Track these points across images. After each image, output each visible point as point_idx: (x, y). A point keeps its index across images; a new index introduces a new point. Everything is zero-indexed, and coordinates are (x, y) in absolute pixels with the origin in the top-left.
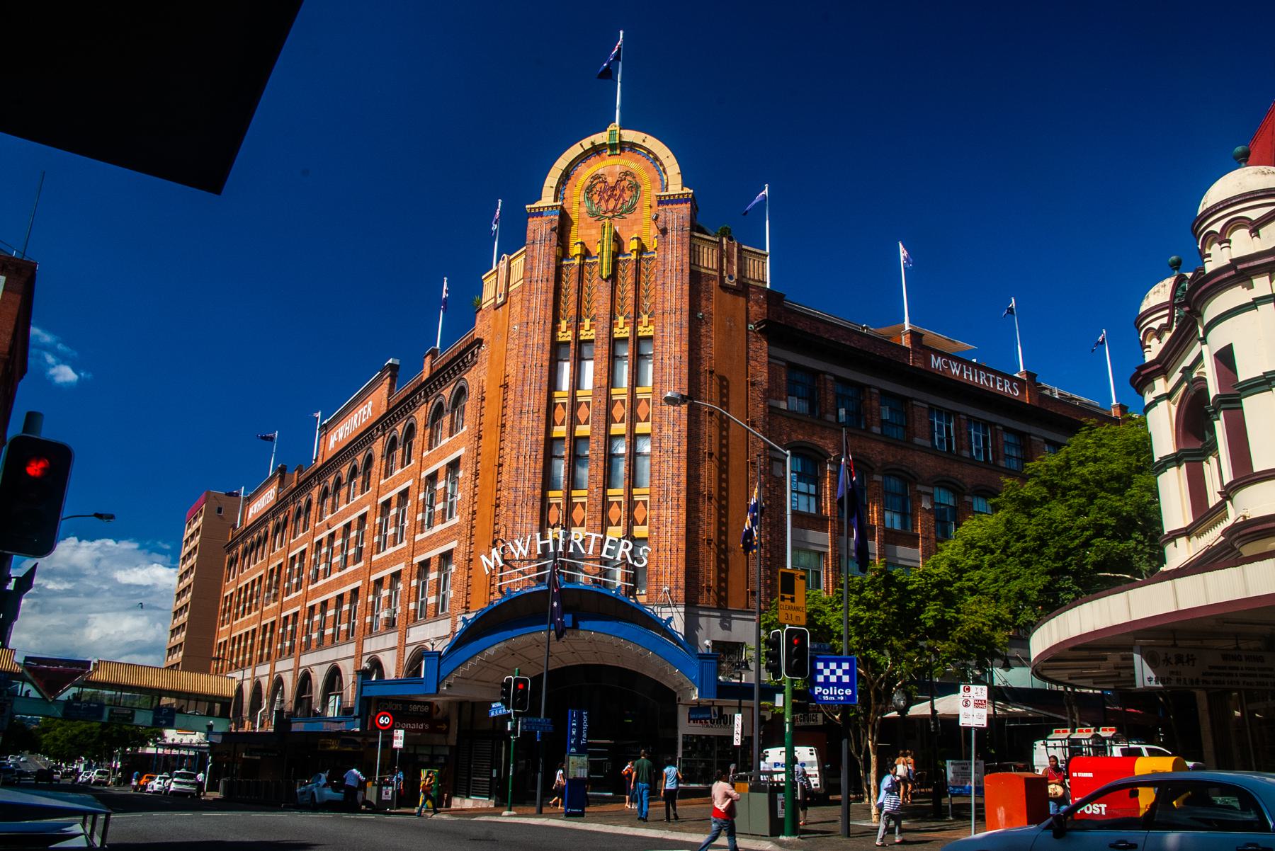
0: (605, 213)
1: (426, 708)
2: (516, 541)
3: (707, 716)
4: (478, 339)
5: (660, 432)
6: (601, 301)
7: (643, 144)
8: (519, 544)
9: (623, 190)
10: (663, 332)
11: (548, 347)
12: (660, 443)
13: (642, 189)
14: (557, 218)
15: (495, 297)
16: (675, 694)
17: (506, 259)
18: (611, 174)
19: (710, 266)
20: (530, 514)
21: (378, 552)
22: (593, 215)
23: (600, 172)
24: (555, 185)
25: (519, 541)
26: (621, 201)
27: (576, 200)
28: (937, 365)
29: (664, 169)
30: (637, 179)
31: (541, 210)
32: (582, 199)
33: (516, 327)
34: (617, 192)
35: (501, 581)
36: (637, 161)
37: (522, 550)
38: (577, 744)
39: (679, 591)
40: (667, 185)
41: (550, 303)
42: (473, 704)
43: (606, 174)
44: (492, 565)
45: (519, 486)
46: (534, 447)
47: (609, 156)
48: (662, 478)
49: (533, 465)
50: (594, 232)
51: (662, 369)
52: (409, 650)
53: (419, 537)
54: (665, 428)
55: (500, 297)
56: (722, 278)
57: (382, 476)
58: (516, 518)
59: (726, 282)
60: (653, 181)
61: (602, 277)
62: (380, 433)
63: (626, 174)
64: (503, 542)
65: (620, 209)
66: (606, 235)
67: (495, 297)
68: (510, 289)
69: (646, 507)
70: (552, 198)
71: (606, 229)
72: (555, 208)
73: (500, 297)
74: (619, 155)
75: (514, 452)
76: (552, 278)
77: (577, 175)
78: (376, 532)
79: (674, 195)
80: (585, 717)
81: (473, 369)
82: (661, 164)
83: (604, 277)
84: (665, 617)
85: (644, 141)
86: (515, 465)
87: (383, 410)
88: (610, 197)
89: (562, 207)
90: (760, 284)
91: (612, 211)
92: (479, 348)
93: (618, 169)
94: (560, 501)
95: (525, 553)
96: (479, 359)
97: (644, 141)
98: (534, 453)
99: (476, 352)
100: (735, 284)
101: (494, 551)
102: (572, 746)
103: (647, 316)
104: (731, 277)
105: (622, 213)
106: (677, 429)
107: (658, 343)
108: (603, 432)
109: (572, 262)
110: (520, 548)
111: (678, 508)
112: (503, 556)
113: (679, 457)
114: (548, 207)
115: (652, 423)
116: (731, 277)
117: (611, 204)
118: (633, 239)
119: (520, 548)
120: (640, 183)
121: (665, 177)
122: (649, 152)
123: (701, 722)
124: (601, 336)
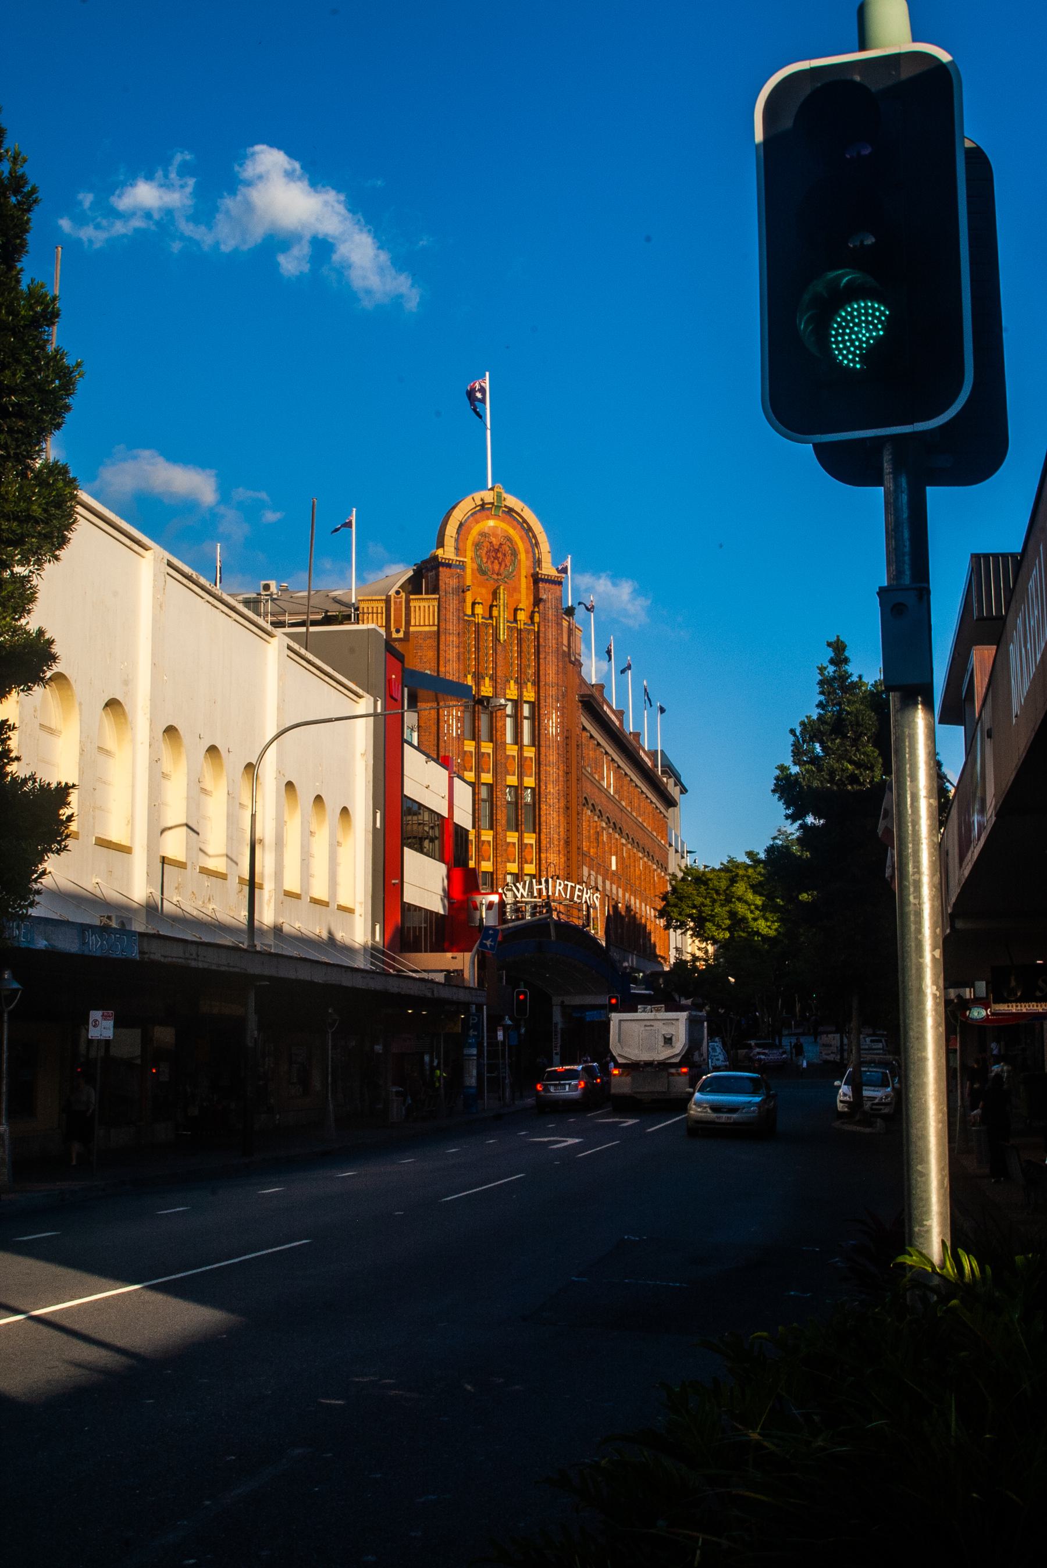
2: (518, 884)
7: (522, 513)
18: (495, 535)
26: (503, 565)
29: (537, 544)
31: (450, 562)
34: (499, 555)
43: (490, 533)
48: (548, 827)
55: (398, 631)
60: (527, 552)
72: (461, 564)
73: (398, 631)
82: (535, 537)
85: (522, 510)
95: (525, 894)
97: (522, 510)
106: (557, 788)
110: (521, 890)
119: (521, 890)
122: (525, 521)
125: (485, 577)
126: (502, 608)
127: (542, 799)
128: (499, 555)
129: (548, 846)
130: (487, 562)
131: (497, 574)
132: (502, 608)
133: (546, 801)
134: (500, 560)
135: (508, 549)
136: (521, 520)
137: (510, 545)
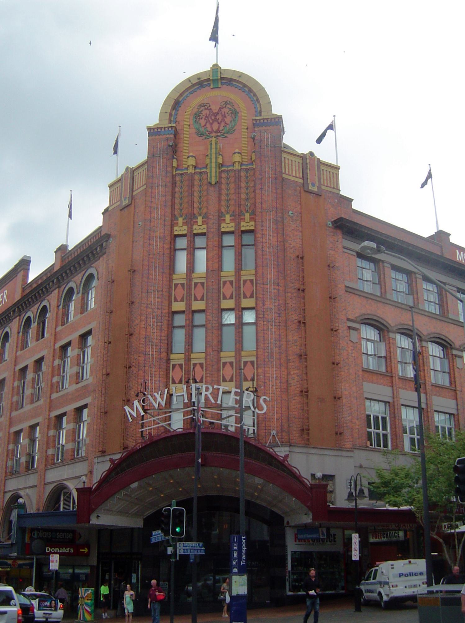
1: (70, 536)
3: (315, 536)
4: (106, 234)
5: (263, 305)
8: (158, 397)
9: (224, 116)
10: (262, 226)
11: (168, 239)
12: (264, 315)
13: (239, 115)
14: (172, 136)
15: (121, 201)
16: (282, 519)
19: (298, 176)
20: (158, 373)
21: (17, 410)
22: (200, 134)
23: (205, 101)
24: (169, 111)
25: (158, 394)
26: (223, 124)
27: (187, 123)
28: (460, 258)
29: (258, 100)
31: (159, 130)
33: (140, 223)
34: (219, 117)
35: (142, 427)
37: (161, 401)
38: (238, 566)
39: (284, 434)
40: (260, 112)
41: (169, 203)
42: (112, 530)
44: (135, 415)
45: (147, 350)
46: (160, 318)
47: (212, 88)
49: (159, 334)
51: (263, 255)
52: (49, 489)
53: (54, 396)
54: (268, 302)
57: (19, 348)
58: (146, 377)
59: (310, 188)
61: (210, 183)
62: (16, 315)
63: (226, 103)
64: (145, 395)
65: (223, 130)
67: (121, 201)
68: (135, 193)
69: (253, 366)
70: (167, 121)
73: (125, 200)
74: (220, 88)
75: (143, 323)
76: (170, 184)
78: (15, 393)
79: (267, 119)
80: (244, 541)
81: (101, 259)
82: (255, 95)
83: (213, 183)
84: (282, 454)
86: (144, 333)
87: (18, 297)
88: (213, 121)
89: (176, 128)
90: (335, 191)
91: (216, 132)
92: (107, 241)
94: (182, 362)
95: (163, 404)
96: (107, 251)
98: (159, 324)
99: (104, 245)
101: (136, 403)
102: (235, 567)
103: (248, 214)
104: (313, 185)
105: (224, 134)
107: (259, 235)
108: (216, 306)
109: (186, 171)
110: (159, 399)
111: (280, 367)
112: (143, 406)
113: (279, 325)
114: (165, 128)
115: (257, 299)
116: (313, 185)
117: (215, 126)
119: (159, 399)
120: (237, 110)
121: (258, 106)
123: (305, 541)
124: (212, 230)
125: (203, 138)
126: (214, 156)
127: (259, 316)
129: (266, 360)
130: (205, 125)
131: (216, 132)
133: (264, 317)
134: (219, 121)
135: (228, 110)
136: (241, 86)
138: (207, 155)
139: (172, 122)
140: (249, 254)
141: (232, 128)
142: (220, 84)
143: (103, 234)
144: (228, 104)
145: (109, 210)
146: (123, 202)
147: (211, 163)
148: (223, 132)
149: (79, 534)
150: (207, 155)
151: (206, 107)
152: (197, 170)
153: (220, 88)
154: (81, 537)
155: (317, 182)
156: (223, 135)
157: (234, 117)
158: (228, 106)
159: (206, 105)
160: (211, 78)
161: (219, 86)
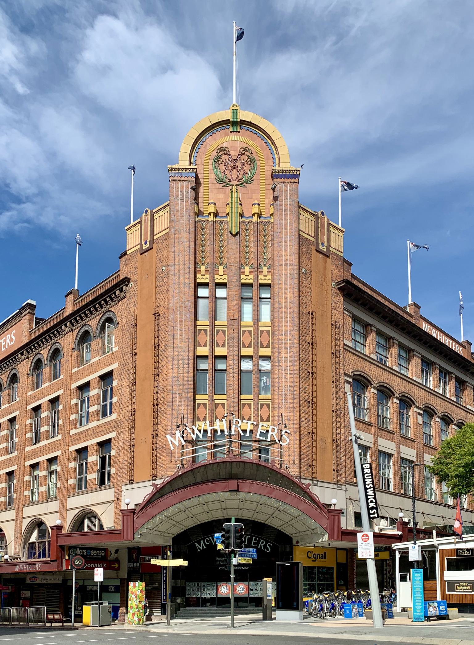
0: (230, 181)
1: (102, 553)
6: (231, 253)
15: (141, 244)
17: (149, 212)
23: (225, 145)
30: (254, 155)
32: (211, 167)
34: (238, 164)
36: (254, 140)
43: (230, 148)
47: (231, 132)
50: (221, 196)
55: (146, 243)
56: (317, 244)
59: (320, 248)
63: (245, 149)
66: (233, 199)
71: (233, 193)
74: (239, 132)
77: (206, 146)
88: (234, 167)
93: (239, 145)
100: (325, 250)
104: (323, 244)
116: (323, 244)
117: (234, 174)
118: (254, 204)
128: (238, 164)
132: (234, 205)
134: (239, 169)
137: (249, 155)
138: (228, 204)
139: (192, 164)
140: (266, 309)
141: (252, 177)
142: (239, 128)
143: (122, 278)
144: (247, 151)
145: (127, 253)
146: (144, 245)
147: (232, 212)
148: (242, 181)
149: (110, 551)
150: (228, 204)
151: (225, 152)
152: (218, 219)
153: (239, 132)
154: (111, 554)
155: (326, 242)
156: (242, 184)
157: (252, 166)
158: (246, 153)
159: (225, 150)
160: (231, 120)
161: (239, 130)
